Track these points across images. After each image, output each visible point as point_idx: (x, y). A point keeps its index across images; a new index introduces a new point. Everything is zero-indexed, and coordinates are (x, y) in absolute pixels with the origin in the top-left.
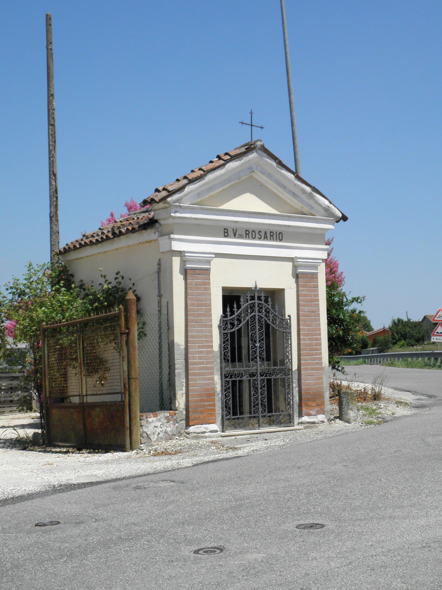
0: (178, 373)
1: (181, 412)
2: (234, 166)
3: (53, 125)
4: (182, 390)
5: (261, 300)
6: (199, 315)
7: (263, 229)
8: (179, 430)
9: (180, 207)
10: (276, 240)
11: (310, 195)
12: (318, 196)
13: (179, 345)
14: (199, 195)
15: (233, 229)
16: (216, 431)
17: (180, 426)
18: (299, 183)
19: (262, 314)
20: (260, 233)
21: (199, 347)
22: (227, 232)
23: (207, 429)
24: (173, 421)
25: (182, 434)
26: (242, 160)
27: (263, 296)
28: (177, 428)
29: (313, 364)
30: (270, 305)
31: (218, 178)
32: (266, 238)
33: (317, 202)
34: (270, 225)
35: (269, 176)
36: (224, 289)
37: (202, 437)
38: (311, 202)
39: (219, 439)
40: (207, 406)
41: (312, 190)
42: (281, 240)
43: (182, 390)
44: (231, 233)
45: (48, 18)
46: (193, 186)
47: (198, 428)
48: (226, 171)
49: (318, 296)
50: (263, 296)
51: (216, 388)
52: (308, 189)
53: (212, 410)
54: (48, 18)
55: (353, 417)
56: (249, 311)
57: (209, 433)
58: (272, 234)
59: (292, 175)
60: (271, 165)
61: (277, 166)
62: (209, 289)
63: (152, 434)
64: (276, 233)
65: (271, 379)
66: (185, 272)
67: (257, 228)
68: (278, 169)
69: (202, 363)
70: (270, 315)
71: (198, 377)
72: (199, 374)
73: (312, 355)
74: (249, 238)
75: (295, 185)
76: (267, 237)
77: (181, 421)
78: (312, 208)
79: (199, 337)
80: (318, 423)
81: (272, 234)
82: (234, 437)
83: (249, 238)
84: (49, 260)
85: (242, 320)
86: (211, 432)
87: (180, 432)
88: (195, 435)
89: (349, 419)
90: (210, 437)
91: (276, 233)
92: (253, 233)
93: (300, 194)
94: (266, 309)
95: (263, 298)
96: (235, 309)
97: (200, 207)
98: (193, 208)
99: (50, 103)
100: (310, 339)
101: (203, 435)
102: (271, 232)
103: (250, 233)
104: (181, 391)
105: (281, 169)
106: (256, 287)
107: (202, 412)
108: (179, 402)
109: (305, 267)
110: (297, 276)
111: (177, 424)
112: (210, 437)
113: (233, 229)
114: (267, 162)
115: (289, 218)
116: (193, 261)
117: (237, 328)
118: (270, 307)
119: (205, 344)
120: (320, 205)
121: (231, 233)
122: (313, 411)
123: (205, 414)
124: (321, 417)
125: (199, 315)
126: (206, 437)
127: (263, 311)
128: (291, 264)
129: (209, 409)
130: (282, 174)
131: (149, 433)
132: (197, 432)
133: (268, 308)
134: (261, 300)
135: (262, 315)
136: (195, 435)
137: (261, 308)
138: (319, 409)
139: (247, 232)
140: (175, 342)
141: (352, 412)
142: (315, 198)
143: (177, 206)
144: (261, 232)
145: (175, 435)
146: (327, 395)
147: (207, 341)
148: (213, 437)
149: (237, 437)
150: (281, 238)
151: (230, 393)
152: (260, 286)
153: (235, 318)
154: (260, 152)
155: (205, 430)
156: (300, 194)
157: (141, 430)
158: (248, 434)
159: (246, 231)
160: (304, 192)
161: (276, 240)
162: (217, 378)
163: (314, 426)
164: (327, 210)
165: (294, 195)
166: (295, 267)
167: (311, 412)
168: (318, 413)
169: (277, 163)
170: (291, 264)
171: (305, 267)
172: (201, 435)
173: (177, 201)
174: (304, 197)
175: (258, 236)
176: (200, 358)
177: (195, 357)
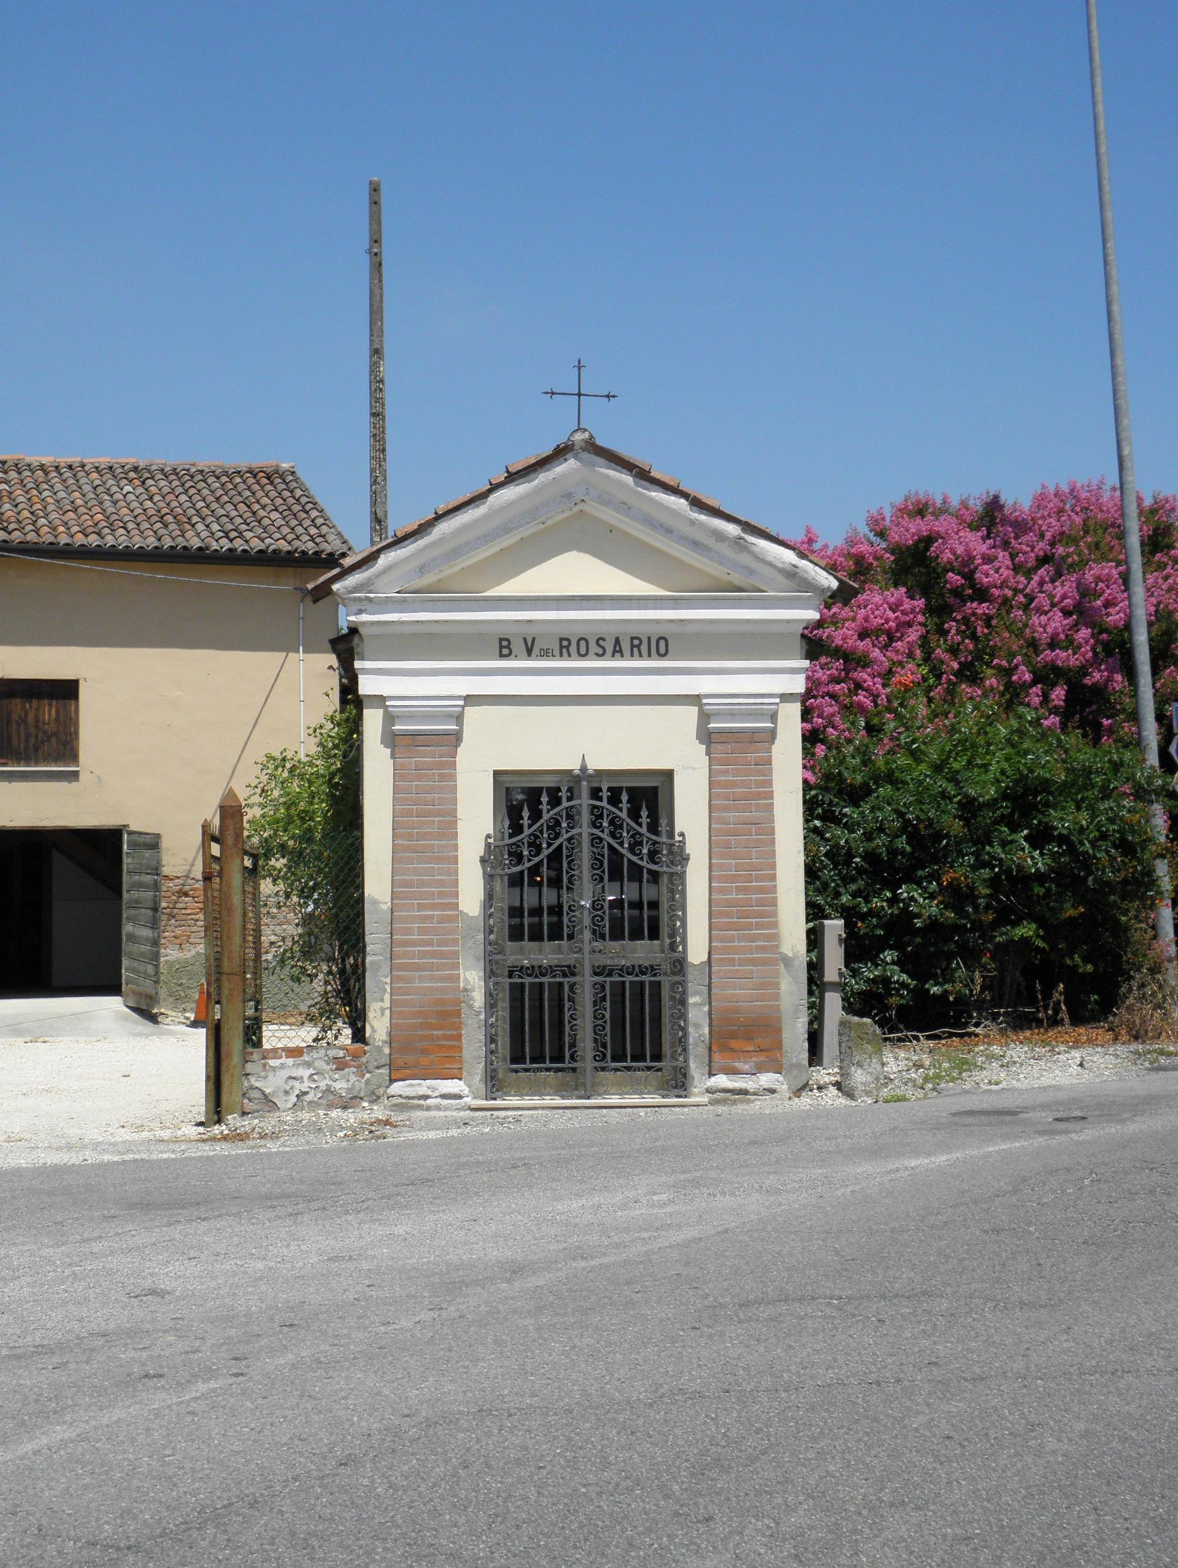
0: (372, 962)
1: (379, 1049)
2: (513, 497)
3: (374, 415)
4: (382, 1000)
5: (600, 799)
6: (421, 836)
7: (610, 632)
8: (371, 1087)
9: (370, 600)
10: (650, 655)
11: (738, 544)
12: (763, 543)
13: (376, 902)
14: (422, 569)
15: (525, 639)
16: (458, 1097)
17: (374, 1081)
18: (703, 518)
19: (602, 831)
20: (601, 642)
21: (421, 907)
22: (508, 647)
23: (434, 1089)
24: (359, 1067)
25: (379, 1097)
26: (534, 480)
27: (605, 790)
28: (367, 1082)
29: (750, 950)
30: (625, 811)
31: (465, 528)
32: (618, 651)
33: (760, 559)
34: (658, 622)
35: (624, 508)
36: (497, 773)
37: (420, 1107)
38: (743, 558)
39: (462, 1114)
40: (439, 1038)
41: (744, 530)
42: (663, 656)
43: (382, 1000)
44: (518, 646)
45: (375, 189)
46: (399, 552)
47: (411, 1085)
48: (490, 509)
49: (771, 786)
50: (605, 790)
51: (473, 999)
52: (732, 529)
53: (452, 1047)
54: (375, 189)
55: (864, 1084)
56: (564, 825)
57: (439, 1100)
58: (636, 642)
59: (683, 501)
60: (619, 483)
61: (636, 484)
62: (453, 778)
63: (282, 1094)
64: (649, 639)
65: (623, 983)
66: (391, 739)
67: (592, 633)
68: (640, 489)
69: (429, 943)
70: (625, 834)
71: (417, 974)
72: (419, 968)
73: (749, 927)
74: (569, 655)
75: (693, 522)
76: (621, 651)
77: (378, 1068)
78: (751, 572)
79: (422, 884)
80: (755, 1094)
81: (636, 642)
82: (489, 1113)
83: (569, 655)
84: (366, 712)
85: (545, 845)
86: (444, 1096)
87: (373, 1093)
88: (401, 1100)
89: (852, 1089)
90: (438, 1108)
91: (649, 639)
92: (583, 643)
93: (711, 542)
94: (613, 819)
95: (605, 794)
96: (525, 822)
97: (431, 594)
98: (404, 600)
99: (374, 367)
100: (739, 890)
101: (422, 1102)
102: (632, 639)
103: (571, 645)
104: (380, 1004)
105: (648, 490)
106: (584, 769)
107: (424, 1052)
108: (372, 1028)
109: (732, 715)
110: (707, 737)
111: (368, 1075)
112: (438, 1108)
113: (525, 639)
114: (608, 477)
115: (675, 603)
116: (410, 717)
117: (527, 865)
118: (624, 815)
119: (437, 901)
120: (771, 565)
121: (518, 646)
122: (745, 1063)
123: (432, 1057)
124: (767, 1079)
125: (421, 836)
126: (428, 1108)
127: (605, 824)
128: (694, 711)
129: (443, 1046)
130: (652, 500)
131: (267, 1091)
132: (405, 1094)
133: (618, 817)
134: (600, 799)
135: (601, 834)
136: (401, 1100)
137: (601, 817)
138: (763, 1059)
139: (565, 643)
140: (366, 895)
141: (860, 1071)
142: (753, 548)
143: (360, 599)
144: (604, 640)
145: (361, 1098)
146: (799, 1025)
147: (441, 895)
148: (446, 1109)
149: (496, 1113)
150: (662, 651)
151: (605, 1009)
152: (593, 765)
153: (525, 841)
154: (585, 456)
155: (429, 1093)
156: (711, 542)
157: (246, 1084)
158: (543, 1108)
159: (561, 640)
160: (720, 536)
161: (650, 655)
162: (472, 979)
163: (742, 1101)
164: (791, 574)
165: (696, 545)
166: (705, 717)
167: (739, 1065)
168: (760, 1069)
169: (635, 476)
170: (694, 711)
171: (732, 715)
172: (416, 1102)
173: (357, 589)
174: (723, 548)
175: (594, 648)
176: (422, 931)
177: (411, 929)
